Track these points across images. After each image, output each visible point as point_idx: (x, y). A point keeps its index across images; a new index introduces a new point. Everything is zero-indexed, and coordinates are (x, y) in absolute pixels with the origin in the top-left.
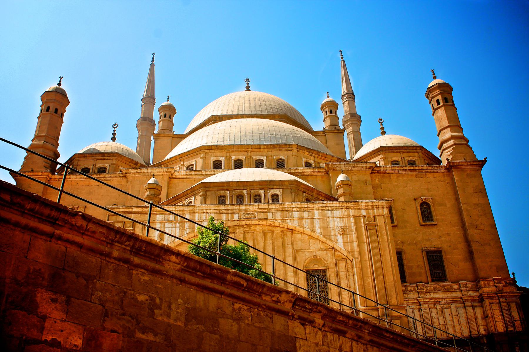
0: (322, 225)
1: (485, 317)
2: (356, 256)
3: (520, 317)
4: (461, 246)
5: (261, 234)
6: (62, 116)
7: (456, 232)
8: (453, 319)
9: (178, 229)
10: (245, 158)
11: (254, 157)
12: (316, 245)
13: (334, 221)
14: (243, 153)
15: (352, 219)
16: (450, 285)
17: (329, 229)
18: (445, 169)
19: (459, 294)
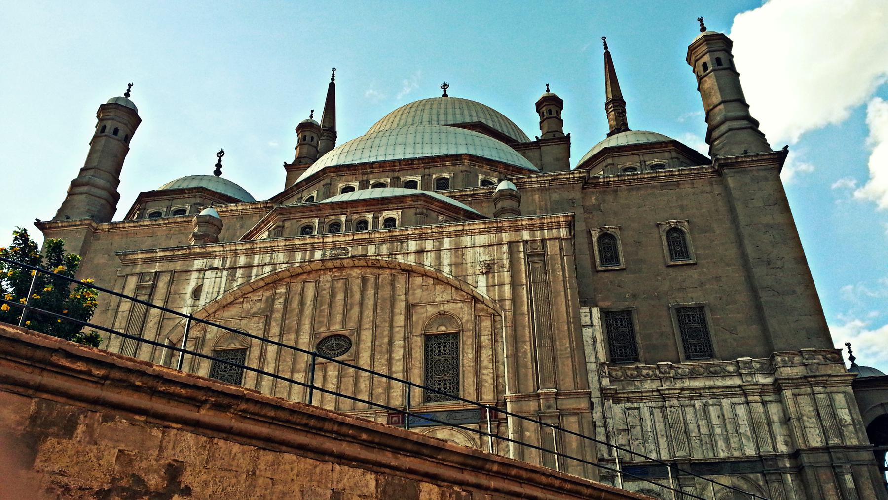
0: (453, 259)
1: (786, 420)
2: (507, 308)
3: (853, 419)
4: (743, 297)
5: (359, 281)
6: (127, 139)
7: (734, 275)
8: (725, 425)
9: (224, 280)
10: (389, 180)
11: (402, 179)
12: (445, 294)
13: (474, 253)
14: (387, 174)
15: (505, 247)
16: (719, 365)
17: (465, 265)
18: (712, 172)
19: (737, 381)
